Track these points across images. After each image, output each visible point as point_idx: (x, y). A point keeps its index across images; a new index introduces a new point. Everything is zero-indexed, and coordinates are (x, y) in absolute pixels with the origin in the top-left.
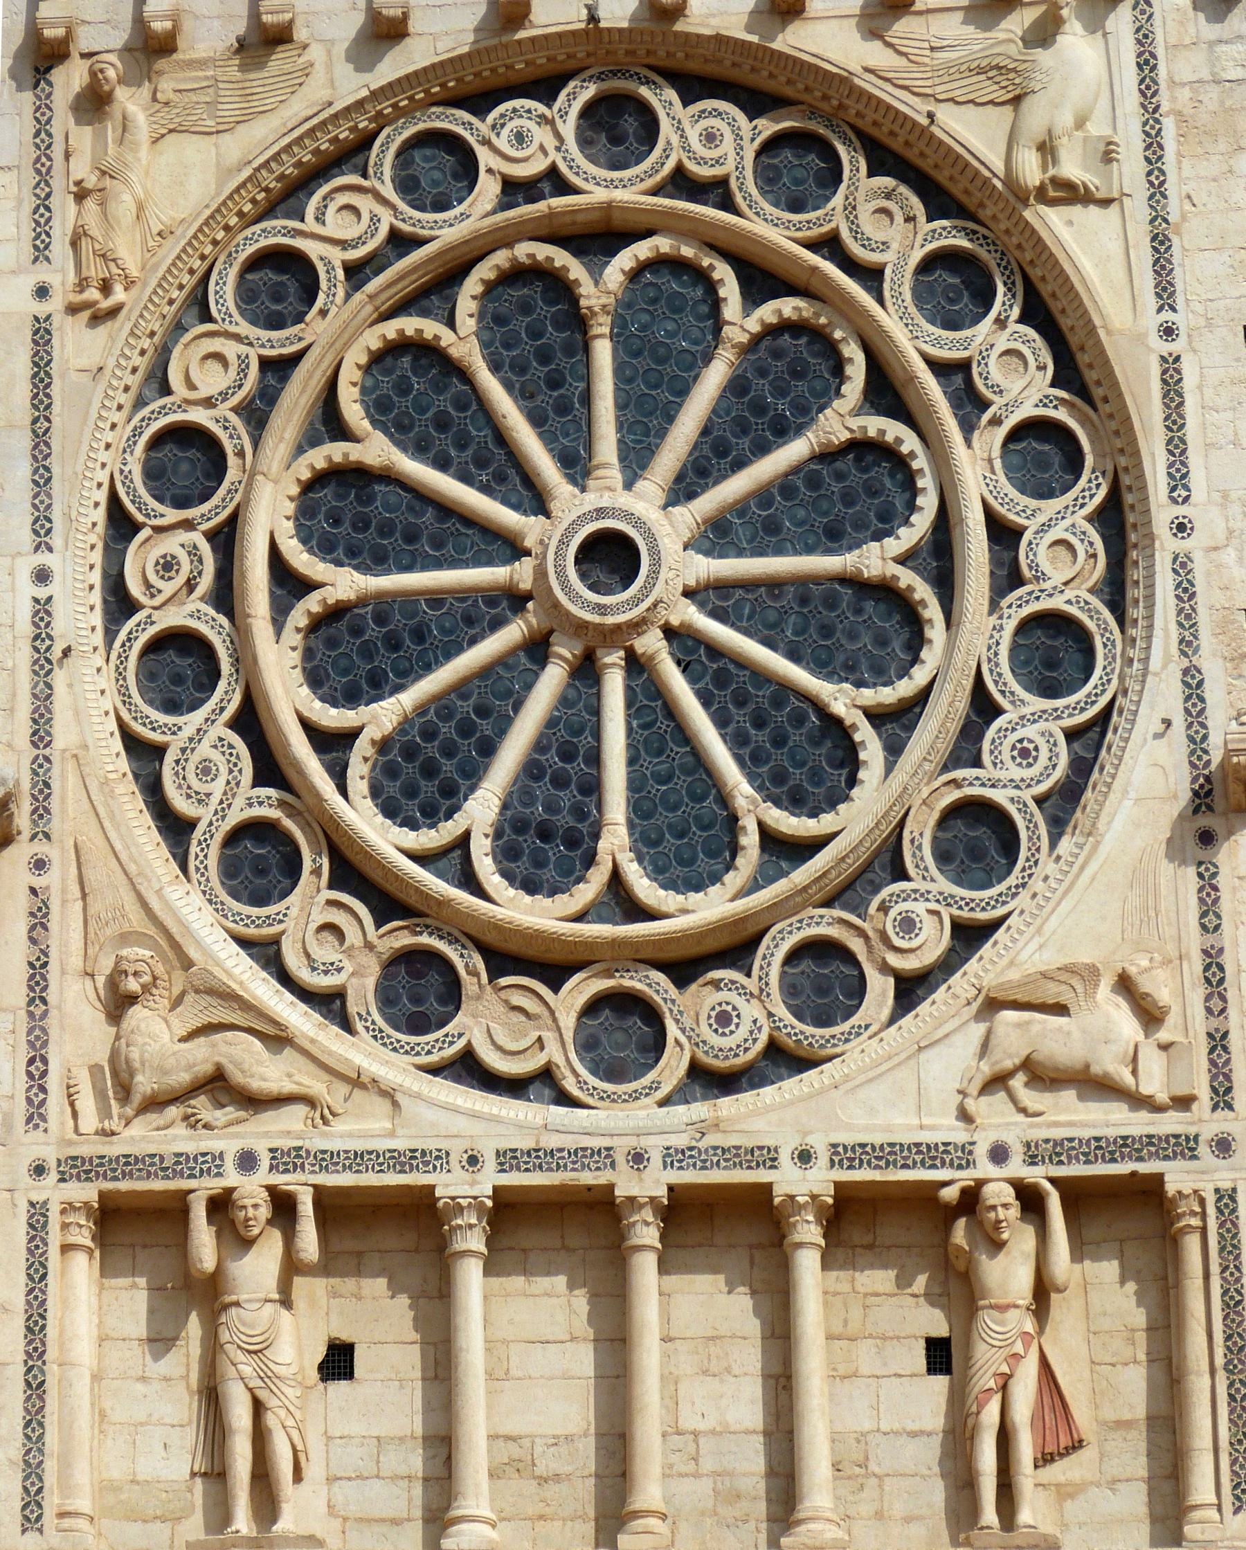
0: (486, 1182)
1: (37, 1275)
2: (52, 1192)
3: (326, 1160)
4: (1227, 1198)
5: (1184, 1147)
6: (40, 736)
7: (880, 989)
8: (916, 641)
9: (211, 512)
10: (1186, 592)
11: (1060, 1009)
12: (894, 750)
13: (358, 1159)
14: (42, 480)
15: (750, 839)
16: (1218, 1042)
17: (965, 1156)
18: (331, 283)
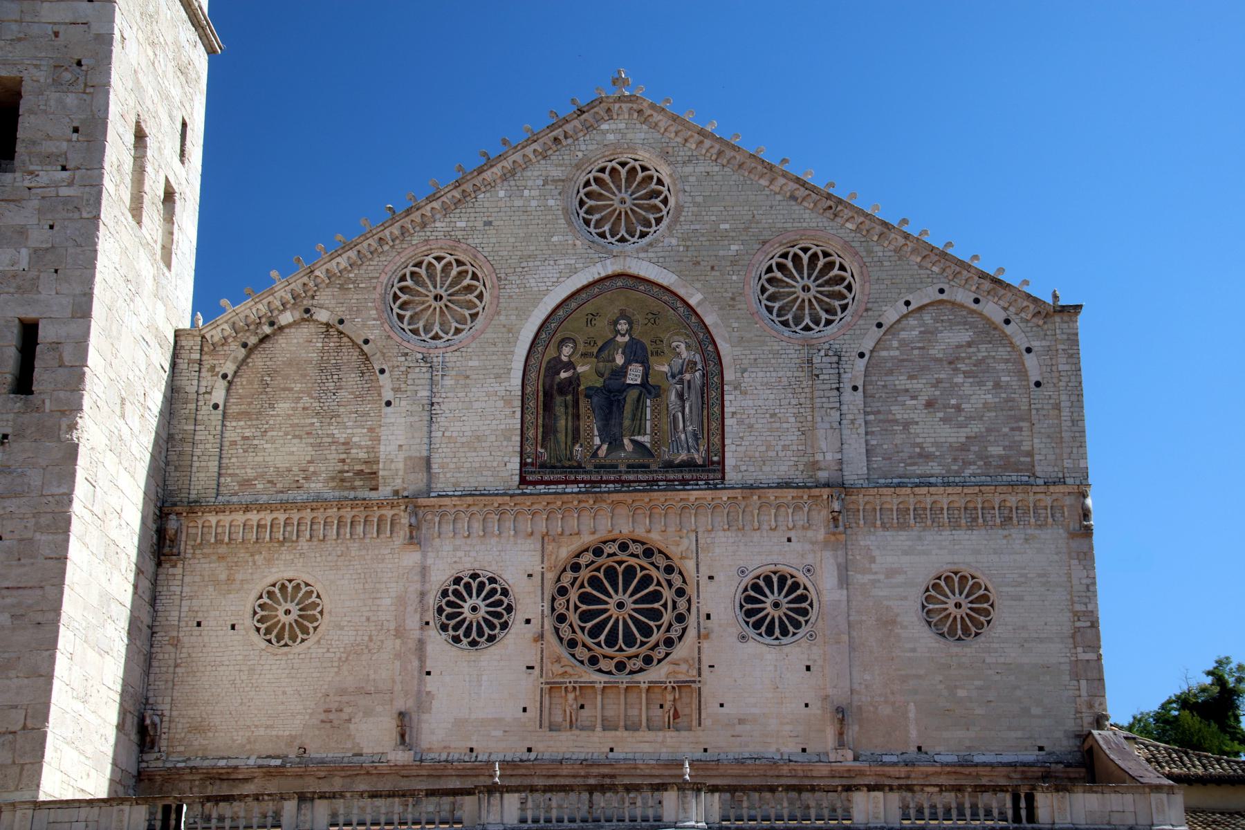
0: (603, 685)
1: (542, 696)
2: (543, 686)
3: (581, 682)
4: (700, 688)
5: (694, 682)
6: (542, 627)
7: (655, 662)
8: (662, 616)
9: (566, 597)
10: (698, 611)
11: (678, 664)
12: (658, 630)
13: (585, 682)
14: (543, 594)
15: (639, 641)
16: (700, 669)
17: (665, 683)
18: (583, 567)
